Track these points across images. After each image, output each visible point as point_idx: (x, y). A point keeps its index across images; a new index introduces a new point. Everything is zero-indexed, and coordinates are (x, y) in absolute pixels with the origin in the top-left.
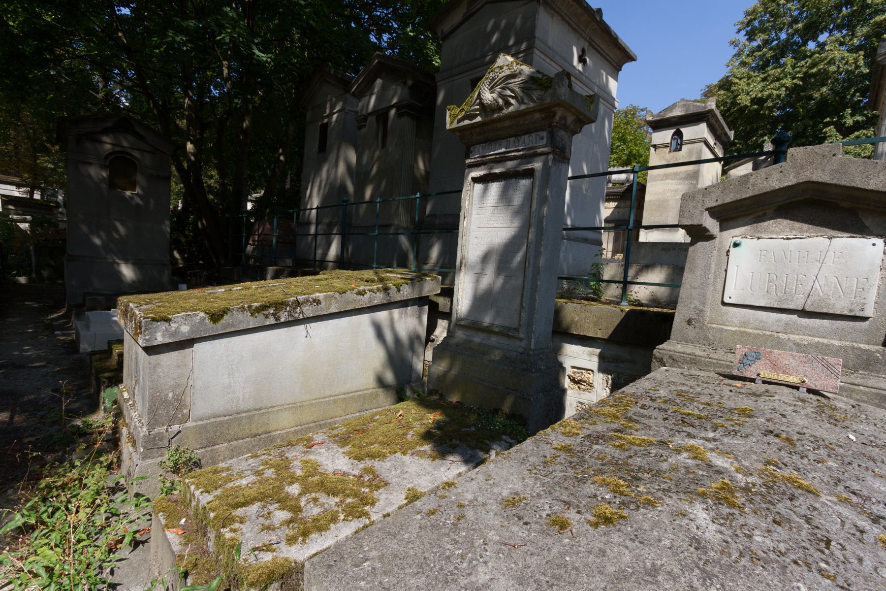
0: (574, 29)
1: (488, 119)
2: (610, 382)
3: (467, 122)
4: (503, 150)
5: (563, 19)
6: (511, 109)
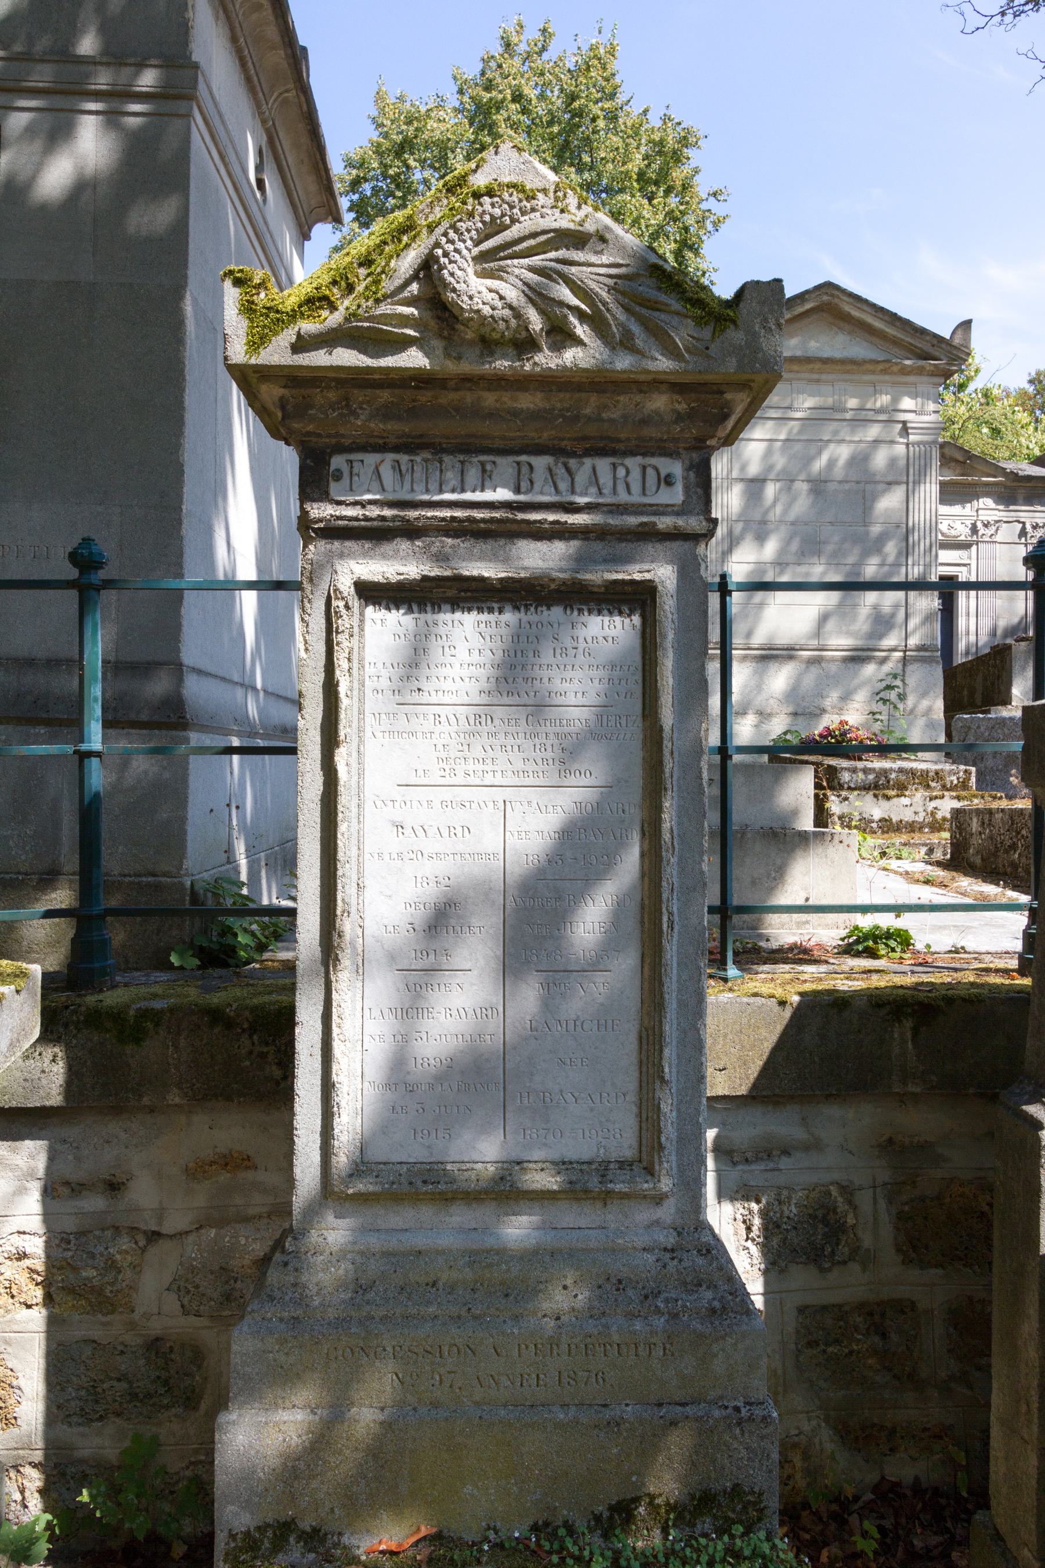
0: (248, 80)
1: (452, 367)
2: (757, 1222)
3: (346, 357)
4: (502, 494)
5: (234, 39)
6: (571, 356)
